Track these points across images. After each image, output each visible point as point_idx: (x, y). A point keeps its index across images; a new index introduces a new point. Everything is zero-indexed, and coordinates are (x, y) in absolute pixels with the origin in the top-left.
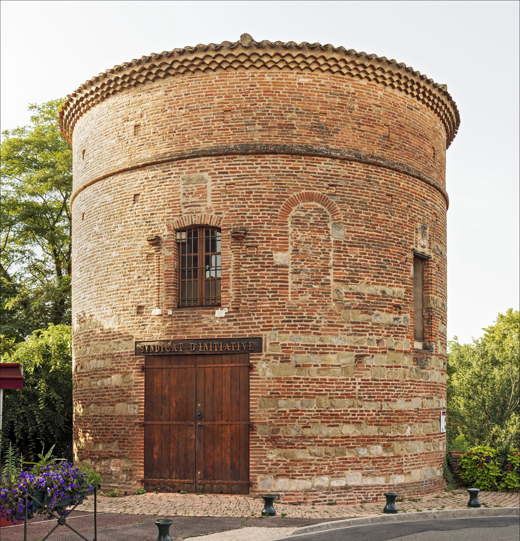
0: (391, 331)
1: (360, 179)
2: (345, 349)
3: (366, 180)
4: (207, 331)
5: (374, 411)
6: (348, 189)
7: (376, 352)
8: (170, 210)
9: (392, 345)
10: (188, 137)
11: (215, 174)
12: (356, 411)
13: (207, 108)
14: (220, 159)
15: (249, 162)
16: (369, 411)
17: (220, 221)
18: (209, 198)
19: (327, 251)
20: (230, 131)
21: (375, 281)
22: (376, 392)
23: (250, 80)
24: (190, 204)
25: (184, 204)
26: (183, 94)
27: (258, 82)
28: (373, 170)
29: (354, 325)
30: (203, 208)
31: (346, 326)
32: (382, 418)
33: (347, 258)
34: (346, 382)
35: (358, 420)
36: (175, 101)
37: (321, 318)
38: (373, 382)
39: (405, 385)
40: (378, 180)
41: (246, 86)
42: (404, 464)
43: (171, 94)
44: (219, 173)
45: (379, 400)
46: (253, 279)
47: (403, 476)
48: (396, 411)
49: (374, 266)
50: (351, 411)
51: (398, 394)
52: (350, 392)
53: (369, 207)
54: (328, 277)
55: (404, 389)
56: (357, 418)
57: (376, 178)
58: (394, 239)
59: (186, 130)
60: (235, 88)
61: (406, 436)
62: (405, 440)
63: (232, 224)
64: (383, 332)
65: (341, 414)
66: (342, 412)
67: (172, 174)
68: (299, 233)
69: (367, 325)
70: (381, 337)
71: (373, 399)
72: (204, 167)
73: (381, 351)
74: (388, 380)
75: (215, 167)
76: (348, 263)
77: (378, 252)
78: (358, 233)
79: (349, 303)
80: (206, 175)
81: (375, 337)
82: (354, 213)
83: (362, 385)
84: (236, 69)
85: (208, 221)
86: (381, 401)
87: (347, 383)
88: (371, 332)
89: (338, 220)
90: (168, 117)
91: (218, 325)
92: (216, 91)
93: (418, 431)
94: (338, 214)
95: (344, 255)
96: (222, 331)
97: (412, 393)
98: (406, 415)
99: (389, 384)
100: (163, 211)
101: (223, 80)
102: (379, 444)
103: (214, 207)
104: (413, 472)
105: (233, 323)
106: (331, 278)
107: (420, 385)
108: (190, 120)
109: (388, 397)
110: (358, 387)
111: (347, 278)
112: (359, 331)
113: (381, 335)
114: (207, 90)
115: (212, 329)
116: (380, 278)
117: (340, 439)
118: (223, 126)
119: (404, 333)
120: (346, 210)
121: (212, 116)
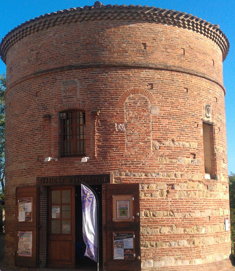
0: (189, 168)
1: (168, 79)
2: (160, 180)
3: (171, 80)
4: (77, 171)
6: (160, 85)
7: (180, 182)
8: (56, 100)
9: (190, 177)
10: (66, 58)
11: (81, 79)
13: (77, 42)
14: (84, 71)
15: (101, 72)
16: (177, 219)
17: (85, 106)
18: (78, 93)
20: (90, 55)
21: (178, 139)
22: (181, 206)
23: (101, 26)
24: (67, 97)
25: (64, 96)
26: (63, 35)
27: (106, 27)
28: (175, 74)
29: (166, 166)
30: (75, 99)
31: (161, 166)
33: (161, 126)
35: (171, 224)
36: (59, 39)
40: (178, 80)
41: (99, 30)
42: (201, 251)
43: (56, 35)
44: (84, 79)
45: (184, 212)
46: (104, 140)
47: (201, 260)
49: (178, 130)
52: (165, 207)
53: (173, 95)
54: (149, 137)
57: (177, 79)
58: (190, 113)
59: (65, 55)
60: (93, 31)
61: (202, 234)
62: (201, 236)
63: (92, 107)
64: (184, 169)
66: (160, 219)
67: (57, 80)
68: (131, 112)
69: (175, 166)
70: (183, 173)
71: (180, 211)
72: (75, 76)
74: (189, 199)
75: (81, 75)
76: (161, 129)
77: (180, 122)
78: (167, 111)
79: (162, 153)
80: (76, 80)
81: (180, 173)
82: (164, 99)
84: (93, 20)
85: (78, 106)
89: (154, 104)
90: (55, 48)
91: (84, 167)
92: (82, 33)
93: (210, 231)
94: (154, 100)
95: (159, 124)
96: (86, 170)
97: (205, 207)
98: (202, 220)
99: (189, 201)
100: (52, 101)
101: (86, 27)
102: (184, 239)
103: (81, 98)
104: (207, 257)
105: (93, 165)
106: (151, 138)
107: (210, 202)
108: (67, 49)
110: (170, 203)
111: (161, 137)
112: (169, 169)
113: (183, 171)
114: (77, 32)
115: (80, 169)
116: (181, 137)
117: (160, 236)
118: (86, 52)
119: (198, 170)
120: (159, 98)
121: (79, 47)
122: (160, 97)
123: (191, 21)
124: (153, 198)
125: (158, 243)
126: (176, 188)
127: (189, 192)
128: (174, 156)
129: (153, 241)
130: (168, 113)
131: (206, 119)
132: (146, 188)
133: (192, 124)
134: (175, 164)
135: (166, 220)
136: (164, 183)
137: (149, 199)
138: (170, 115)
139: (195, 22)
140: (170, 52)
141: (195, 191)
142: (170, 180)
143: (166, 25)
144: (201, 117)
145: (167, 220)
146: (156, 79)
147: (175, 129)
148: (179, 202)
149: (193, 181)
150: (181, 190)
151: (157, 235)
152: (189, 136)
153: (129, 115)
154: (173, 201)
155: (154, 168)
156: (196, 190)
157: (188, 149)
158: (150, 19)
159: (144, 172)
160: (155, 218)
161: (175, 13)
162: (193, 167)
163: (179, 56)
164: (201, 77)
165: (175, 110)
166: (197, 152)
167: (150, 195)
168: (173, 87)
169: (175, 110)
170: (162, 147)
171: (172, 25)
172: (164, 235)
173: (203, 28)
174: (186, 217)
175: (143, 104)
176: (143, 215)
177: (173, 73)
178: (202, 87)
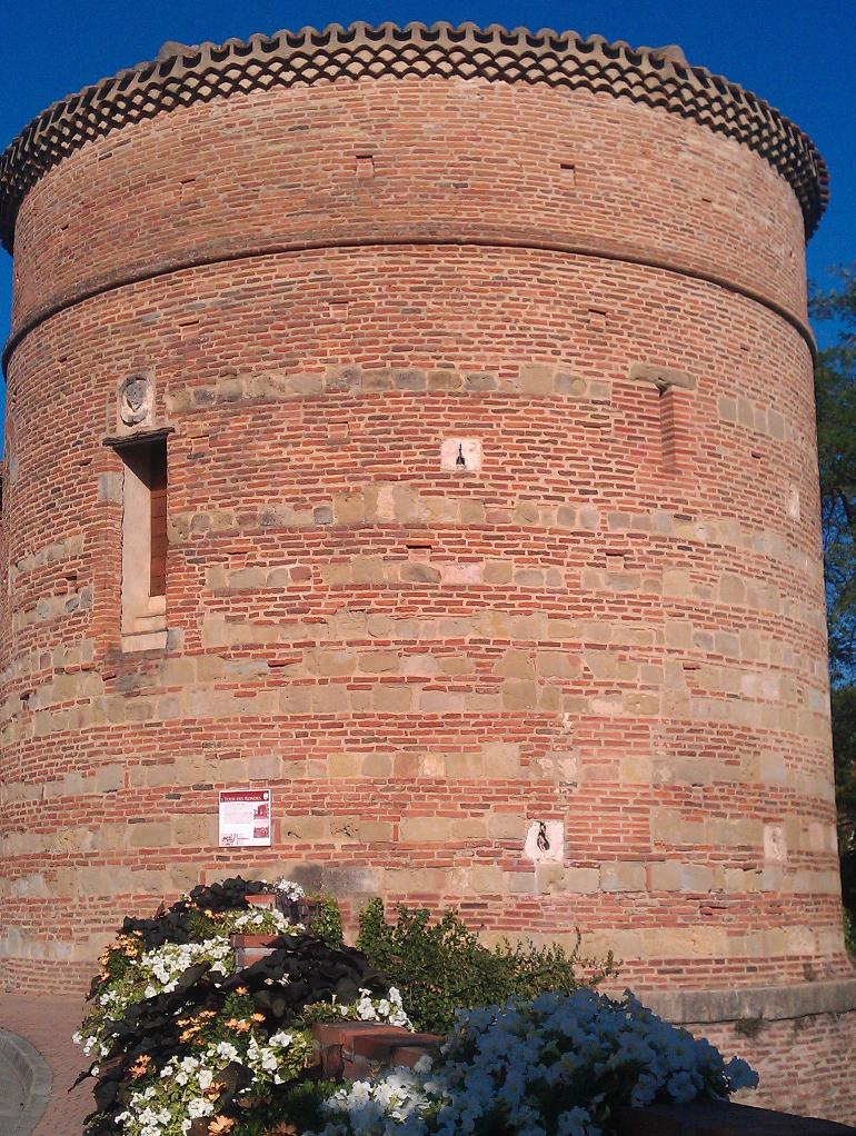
131: (124, 432)
144: (103, 436)
166: (82, 566)
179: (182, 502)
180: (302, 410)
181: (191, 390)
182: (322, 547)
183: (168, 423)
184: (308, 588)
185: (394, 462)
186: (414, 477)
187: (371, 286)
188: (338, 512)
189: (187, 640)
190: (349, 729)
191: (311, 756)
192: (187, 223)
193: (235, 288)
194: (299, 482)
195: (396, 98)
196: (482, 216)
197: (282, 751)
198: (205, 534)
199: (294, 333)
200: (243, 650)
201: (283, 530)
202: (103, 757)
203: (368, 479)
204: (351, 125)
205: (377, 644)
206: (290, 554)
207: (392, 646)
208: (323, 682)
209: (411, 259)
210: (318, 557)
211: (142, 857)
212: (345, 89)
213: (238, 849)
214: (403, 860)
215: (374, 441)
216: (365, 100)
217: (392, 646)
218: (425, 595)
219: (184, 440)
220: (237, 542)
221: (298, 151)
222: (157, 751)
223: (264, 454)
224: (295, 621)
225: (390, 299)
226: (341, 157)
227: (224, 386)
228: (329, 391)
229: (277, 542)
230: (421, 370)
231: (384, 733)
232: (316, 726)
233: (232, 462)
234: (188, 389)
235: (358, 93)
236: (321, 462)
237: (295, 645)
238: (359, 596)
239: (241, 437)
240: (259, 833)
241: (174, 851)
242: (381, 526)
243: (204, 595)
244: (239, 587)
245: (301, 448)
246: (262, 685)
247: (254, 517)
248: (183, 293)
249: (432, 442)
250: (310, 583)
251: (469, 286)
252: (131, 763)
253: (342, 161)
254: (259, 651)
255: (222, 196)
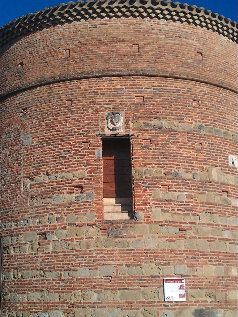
0: (71, 208)
1: (43, 97)
2: (30, 229)
5: (53, 280)
7: (56, 229)
9: (72, 221)
12: (39, 281)
16: (49, 280)
19: (20, 157)
21: (54, 170)
22: (55, 263)
29: (37, 209)
32: (62, 286)
33: (33, 158)
34: (30, 256)
35: (40, 288)
37: (15, 208)
38: (53, 254)
39: (88, 254)
45: (59, 270)
48: (77, 279)
50: (35, 281)
51: (79, 263)
52: (34, 265)
53: (50, 114)
54: (20, 176)
55: (88, 259)
56: (39, 287)
61: (91, 303)
62: (89, 306)
64: (62, 210)
65: (27, 284)
66: (28, 282)
68: (6, 150)
70: (60, 215)
71: (53, 269)
73: (60, 227)
74: (68, 252)
79: (33, 193)
81: (55, 216)
82: (38, 123)
83: (44, 258)
86: (61, 270)
87: (32, 258)
88: (51, 212)
98: (91, 282)
99: (69, 255)
102: (58, 309)
107: (113, 253)
109: (68, 267)
110: (40, 259)
111: (32, 173)
112: (40, 213)
113: (60, 213)
119: (87, 208)
120: (32, 123)
122: (34, 122)
123: (71, 10)
124: (22, 253)
125: (24, 313)
126: (48, 236)
127: (69, 242)
128: (47, 194)
129: (20, 310)
130: (41, 139)
132: (15, 242)
133: (77, 146)
134: (49, 206)
135: (34, 282)
136: (34, 232)
137: (17, 256)
138: (44, 141)
139: (79, 9)
140: (49, 61)
141: (80, 239)
142: (41, 228)
143: (45, 30)
144: (97, 133)
145: (36, 282)
146: (30, 101)
147: (50, 158)
148: (53, 257)
149: (77, 226)
150: (56, 239)
151: (24, 303)
152: (72, 163)
153: (4, 153)
154: (45, 256)
155: (23, 214)
156: (82, 238)
157: (70, 181)
158: (27, 33)
159: (14, 221)
160: (22, 280)
161: (47, 12)
162: (77, 205)
163: (60, 62)
164: (97, 77)
165: (51, 134)
166: (86, 183)
167: (18, 249)
168: (51, 103)
169: (51, 134)
170: (33, 185)
171: (52, 27)
172: (32, 303)
173: (99, 11)
174: (63, 277)
175: (16, 136)
176: (12, 277)
177: (51, 86)
178: (99, 91)
179: (140, 163)
180: (187, 137)
181: (142, 122)
182: (196, 187)
183: (131, 132)
184: (192, 202)
185: (215, 160)
186: (222, 166)
187: (205, 97)
188: (201, 175)
189: (145, 217)
190: (209, 257)
191: (197, 266)
192: (136, 60)
193: (158, 87)
194: (187, 162)
195: (207, 36)
196: (231, 82)
197: (187, 264)
198: (151, 177)
199: (182, 108)
200: (169, 223)
201: (182, 179)
202: (103, 262)
203: (209, 165)
204: (195, 41)
205: (216, 225)
206: (185, 188)
207: (220, 227)
208: (200, 238)
209: (215, 90)
210: (195, 191)
211: (127, 304)
212: (193, 28)
213: (172, 302)
214: (229, 307)
215: (210, 152)
216: (199, 34)
217: (220, 227)
218: (228, 209)
219: (140, 140)
220: (165, 181)
221: (178, 44)
222: (132, 261)
223: (173, 150)
224: (188, 214)
225: (211, 103)
226: (193, 51)
227: (154, 122)
228: (194, 131)
229: (180, 183)
230: (221, 129)
231: (221, 259)
232: (198, 255)
233: (161, 151)
234: (140, 121)
235: (197, 31)
236: (194, 156)
237: (190, 223)
238: (209, 207)
239: (164, 142)
240: (181, 296)
241: (143, 302)
242: (215, 182)
243: (152, 200)
244: (166, 199)
245: (187, 150)
246: (177, 237)
247: (171, 173)
248: (136, 85)
249: (226, 155)
250: (193, 200)
251: (230, 104)
252: (118, 265)
253: (193, 52)
254: (176, 224)
255: (151, 53)
